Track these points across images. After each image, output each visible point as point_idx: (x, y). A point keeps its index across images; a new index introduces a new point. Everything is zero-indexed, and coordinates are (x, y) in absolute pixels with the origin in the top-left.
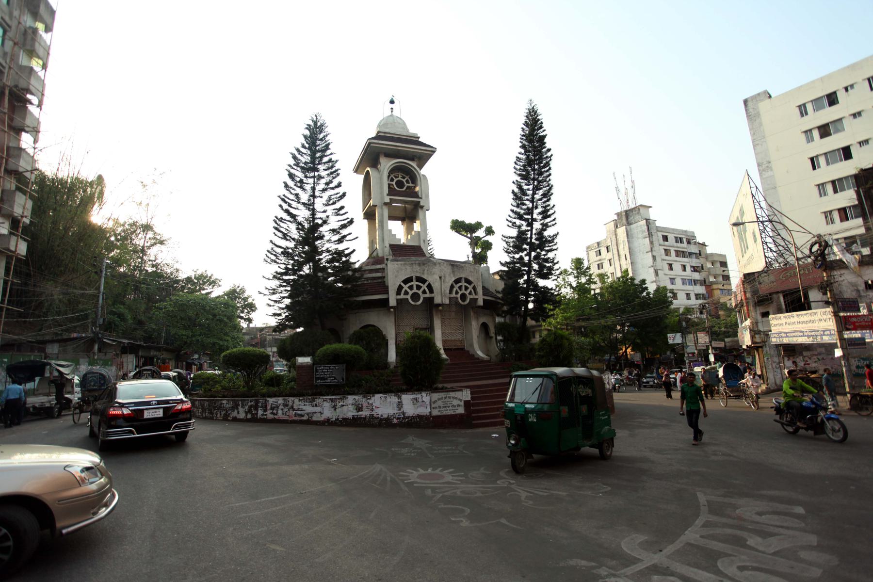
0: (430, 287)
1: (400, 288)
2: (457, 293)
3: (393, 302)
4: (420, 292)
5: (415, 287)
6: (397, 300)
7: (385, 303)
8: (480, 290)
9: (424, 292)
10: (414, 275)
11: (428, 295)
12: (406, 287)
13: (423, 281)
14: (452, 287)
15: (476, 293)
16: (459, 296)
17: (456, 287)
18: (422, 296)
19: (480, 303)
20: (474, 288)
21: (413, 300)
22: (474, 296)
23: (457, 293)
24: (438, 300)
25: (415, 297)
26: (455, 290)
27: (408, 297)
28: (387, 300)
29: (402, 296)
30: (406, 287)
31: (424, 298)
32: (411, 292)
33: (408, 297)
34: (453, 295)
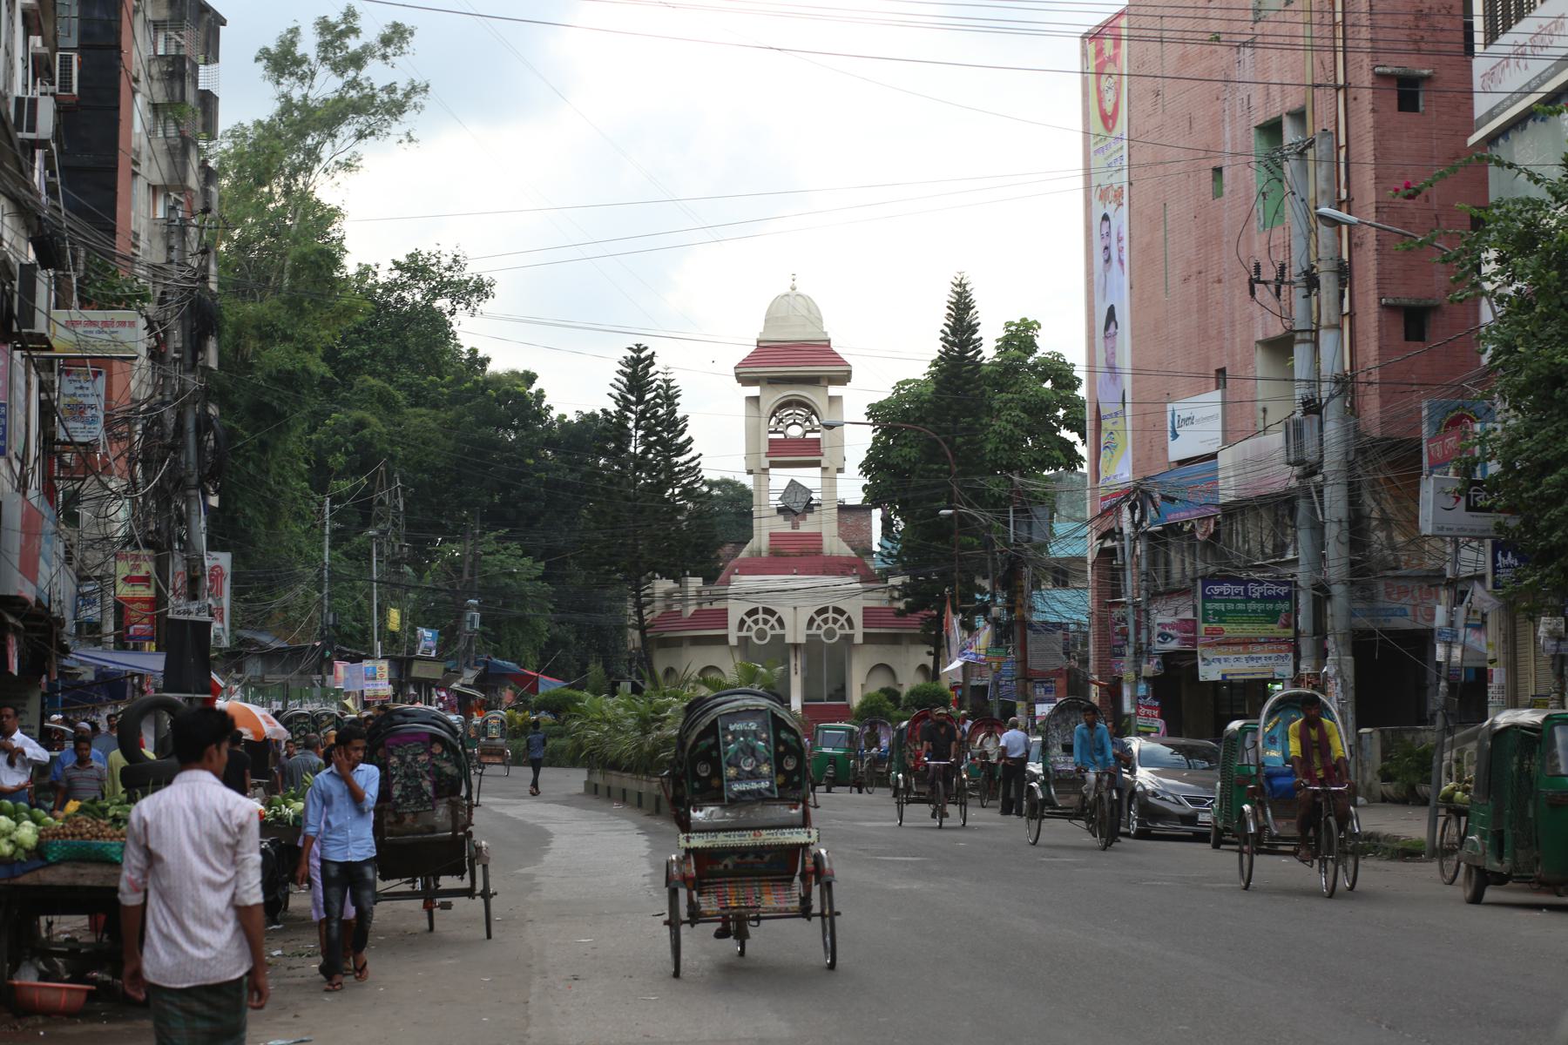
0: (780, 621)
1: (742, 622)
2: (819, 627)
3: (733, 641)
4: (767, 628)
5: (761, 622)
6: (739, 638)
7: (723, 640)
8: (858, 621)
9: (772, 627)
10: (760, 606)
11: (778, 631)
12: (749, 621)
13: (771, 612)
14: (811, 621)
15: (851, 626)
16: (821, 632)
17: (819, 620)
18: (770, 633)
19: (859, 639)
20: (849, 620)
21: (759, 638)
22: (847, 631)
23: (819, 627)
24: (789, 639)
25: (761, 634)
26: (815, 624)
27: (752, 634)
28: (726, 636)
29: (744, 633)
30: (749, 621)
31: (772, 636)
32: (755, 628)
33: (752, 634)
34: (814, 631)
